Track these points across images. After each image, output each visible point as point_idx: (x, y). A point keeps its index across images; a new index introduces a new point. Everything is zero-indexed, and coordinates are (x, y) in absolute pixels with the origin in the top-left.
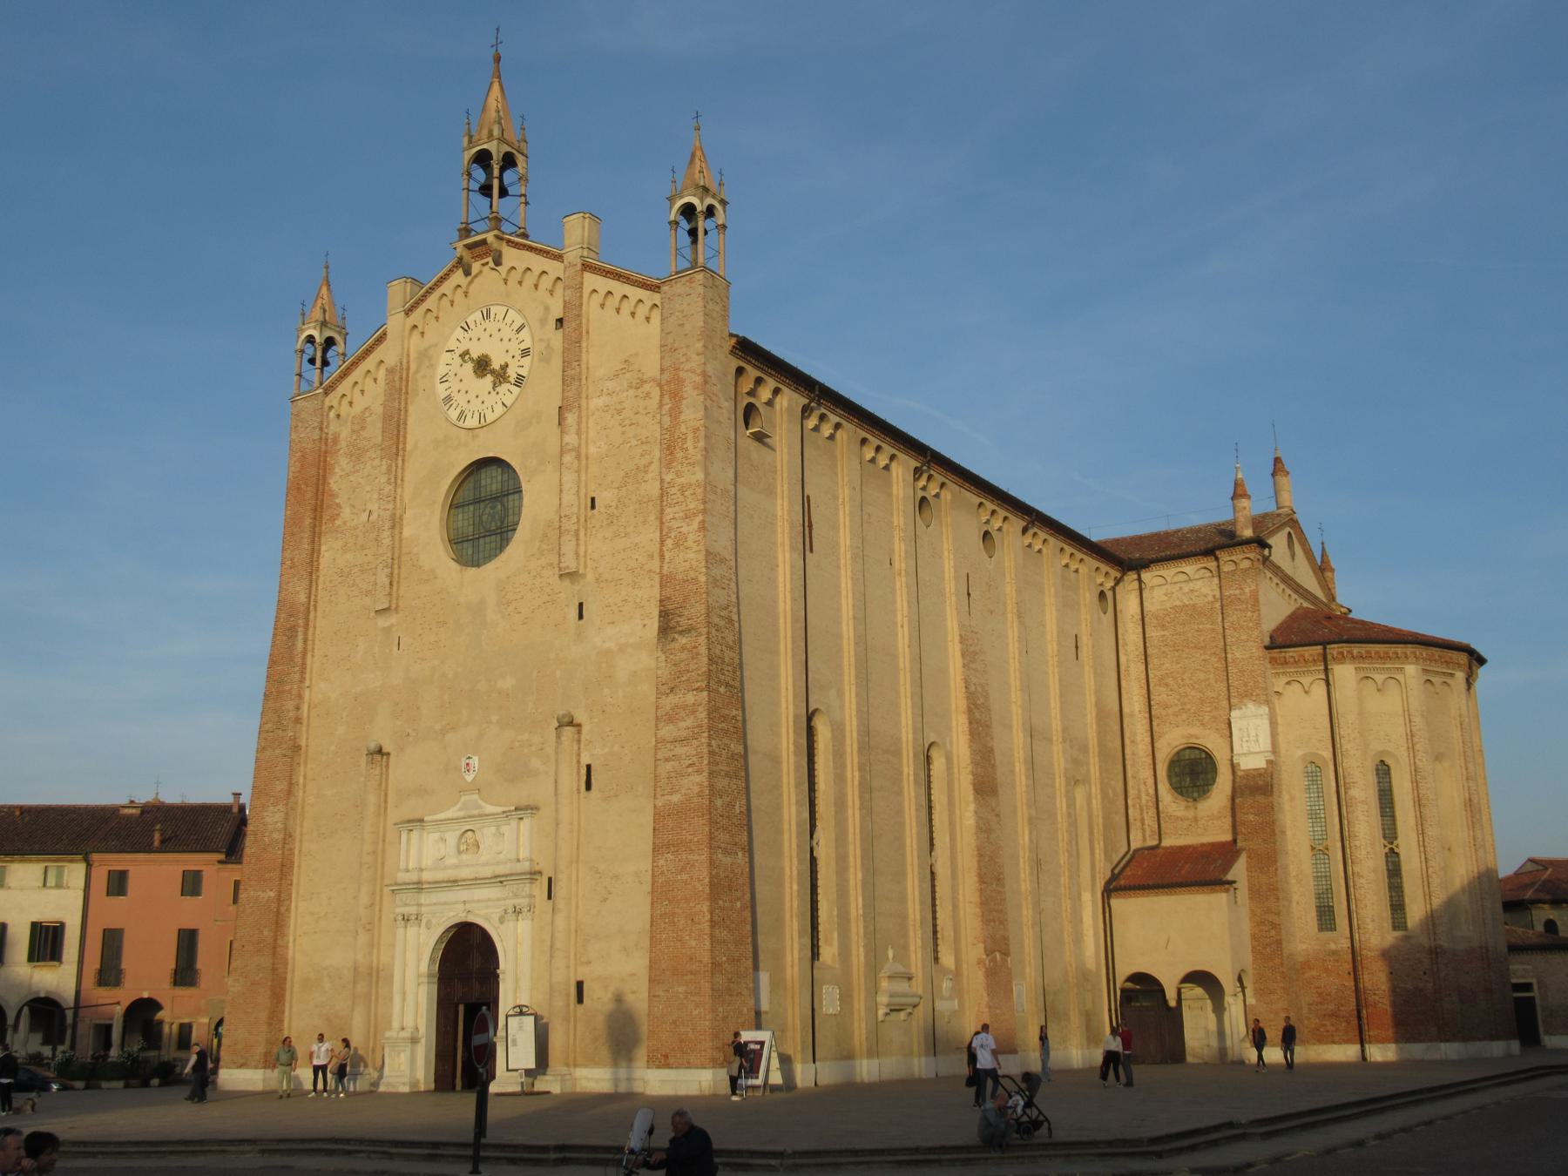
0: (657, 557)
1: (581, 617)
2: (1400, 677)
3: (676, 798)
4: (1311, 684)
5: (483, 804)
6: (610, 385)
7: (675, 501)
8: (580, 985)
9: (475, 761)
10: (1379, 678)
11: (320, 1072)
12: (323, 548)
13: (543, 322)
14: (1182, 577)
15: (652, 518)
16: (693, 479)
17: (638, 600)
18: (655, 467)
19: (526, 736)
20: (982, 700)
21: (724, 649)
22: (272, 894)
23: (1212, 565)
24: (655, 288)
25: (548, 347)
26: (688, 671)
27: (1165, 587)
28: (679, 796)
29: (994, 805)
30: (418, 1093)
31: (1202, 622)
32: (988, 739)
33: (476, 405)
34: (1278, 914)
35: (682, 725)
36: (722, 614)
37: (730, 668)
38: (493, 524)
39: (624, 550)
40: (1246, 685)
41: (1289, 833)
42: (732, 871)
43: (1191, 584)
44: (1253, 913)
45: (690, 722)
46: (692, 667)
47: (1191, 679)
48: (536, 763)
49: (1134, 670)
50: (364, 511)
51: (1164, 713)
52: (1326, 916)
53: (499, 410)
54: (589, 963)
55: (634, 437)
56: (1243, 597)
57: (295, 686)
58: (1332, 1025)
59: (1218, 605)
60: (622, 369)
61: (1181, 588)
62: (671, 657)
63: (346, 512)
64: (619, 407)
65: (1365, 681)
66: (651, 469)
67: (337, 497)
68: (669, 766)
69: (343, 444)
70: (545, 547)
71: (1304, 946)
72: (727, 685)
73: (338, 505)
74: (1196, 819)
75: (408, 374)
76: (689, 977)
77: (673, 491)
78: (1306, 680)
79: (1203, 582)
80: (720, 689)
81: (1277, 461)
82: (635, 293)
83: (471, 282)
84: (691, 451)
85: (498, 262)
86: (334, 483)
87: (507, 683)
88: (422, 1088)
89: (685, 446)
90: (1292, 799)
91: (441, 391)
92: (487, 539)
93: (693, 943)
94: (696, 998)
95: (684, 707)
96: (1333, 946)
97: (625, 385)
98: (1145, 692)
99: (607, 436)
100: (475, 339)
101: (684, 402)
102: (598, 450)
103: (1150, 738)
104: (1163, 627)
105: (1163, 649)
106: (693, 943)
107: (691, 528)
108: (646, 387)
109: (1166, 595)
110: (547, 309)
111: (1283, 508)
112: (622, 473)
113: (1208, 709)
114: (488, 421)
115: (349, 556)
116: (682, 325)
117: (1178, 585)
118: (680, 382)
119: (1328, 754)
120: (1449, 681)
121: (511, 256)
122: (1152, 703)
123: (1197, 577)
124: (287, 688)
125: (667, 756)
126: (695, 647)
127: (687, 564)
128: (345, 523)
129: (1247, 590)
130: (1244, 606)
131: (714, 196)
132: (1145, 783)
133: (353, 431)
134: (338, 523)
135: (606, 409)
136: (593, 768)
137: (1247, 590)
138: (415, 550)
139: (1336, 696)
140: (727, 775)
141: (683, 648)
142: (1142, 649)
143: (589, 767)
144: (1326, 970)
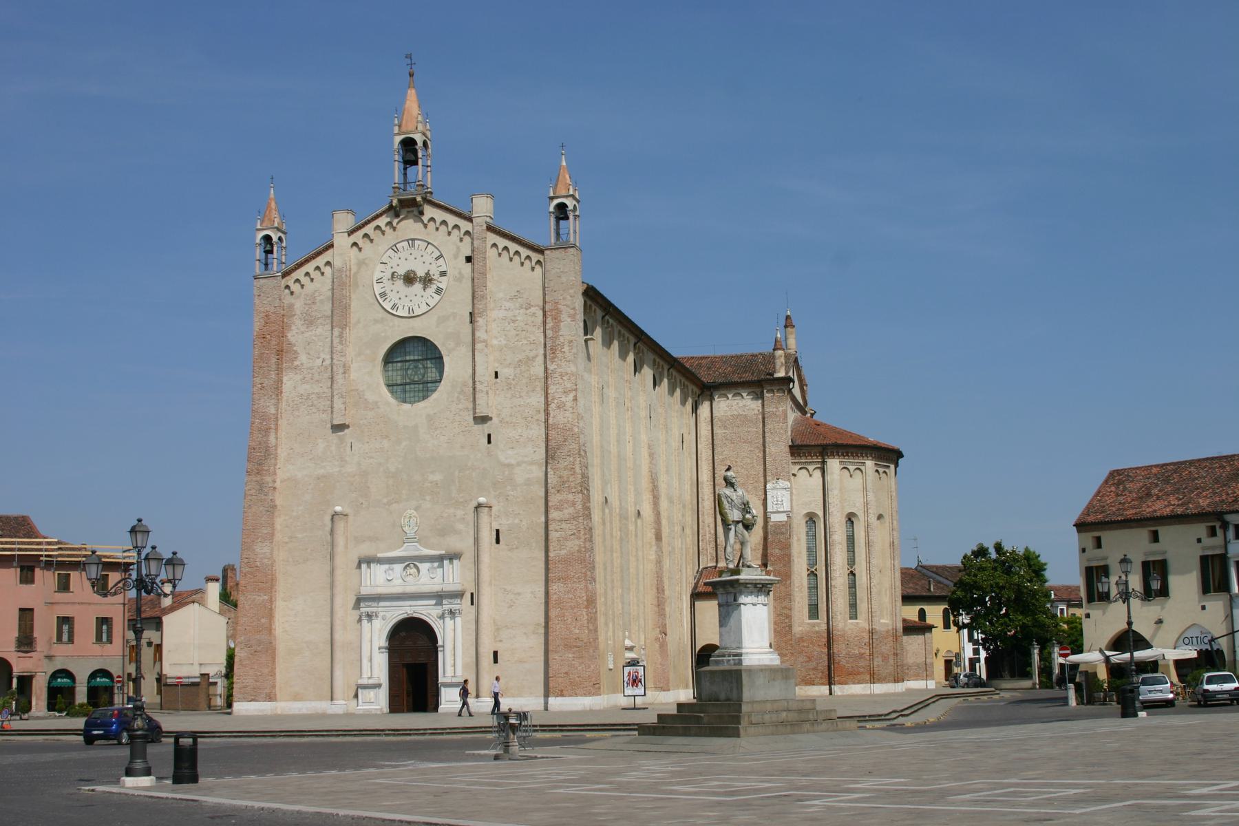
0: (543, 414)
1: (489, 442)
2: (863, 468)
3: (563, 552)
4: (814, 470)
5: (421, 548)
6: (508, 304)
8: (495, 654)
10: (852, 468)
11: (14, 711)
12: (285, 379)
13: (456, 257)
15: (538, 389)
16: (569, 370)
18: (540, 359)
19: (452, 510)
22: (266, 597)
24: (541, 251)
25: (460, 273)
28: (565, 551)
30: (383, 714)
33: (406, 302)
34: (790, 609)
35: (566, 511)
38: (416, 377)
39: (519, 406)
41: (796, 560)
45: (571, 510)
46: (571, 479)
48: (460, 526)
49: (705, 453)
50: (318, 358)
52: (814, 612)
53: (424, 308)
54: (501, 641)
55: (525, 338)
56: (777, 413)
57: (272, 468)
58: (814, 674)
59: (760, 417)
60: (515, 296)
61: (738, 404)
62: (557, 472)
63: (303, 358)
64: (513, 318)
65: (844, 470)
66: (537, 359)
67: (295, 346)
68: (558, 535)
69: (298, 312)
70: (461, 397)
71: (801, 628)
73: (296, 352)
75: (350, 273)
76: (576, 649)
77: (556, 375)
78: (811, 468)
81: (788, 317)
82: (525, 252)
84: (567, 354)
85: (422, 213)
86: (291, 336)
87: (437, 477)
88: (385, 712)
89: (563, 350)
90: (799, 540)
91: (378, 289)
92: (412, 386)
93: (577, 631)
94: (580, 661)
95: (567, 502)
96: (817, 628)
97: (518, 305)
98: (711, 468)
99: (505, 335)
100: (403, 259)
101: (562, 324)
102: (500, 343)
103: (713, 498)
104: (725, 428)
105: (724, 442)
106: (577, 631)
108: (533, 310)
110: (458, 248)
111: (790, 349)
112: (517, 359)
114: (416, 314)
115: (307, 386)
118: (559, 311)
119: (821, 514)
120: (887, 470)
121: (429, 212)
124: (266, 468)
125: (557, 528)
128: (302, 364)
129: (781, 409)
132: (709, 526)
133: (305, 304)
134: (296, 363)
135: (504, 319)
136: (500, 531)
137: (781, 409)
138: (361, 389)
139: (829, 478)
142: (711, 441)
143: (498, 531)
144: (812, 643)
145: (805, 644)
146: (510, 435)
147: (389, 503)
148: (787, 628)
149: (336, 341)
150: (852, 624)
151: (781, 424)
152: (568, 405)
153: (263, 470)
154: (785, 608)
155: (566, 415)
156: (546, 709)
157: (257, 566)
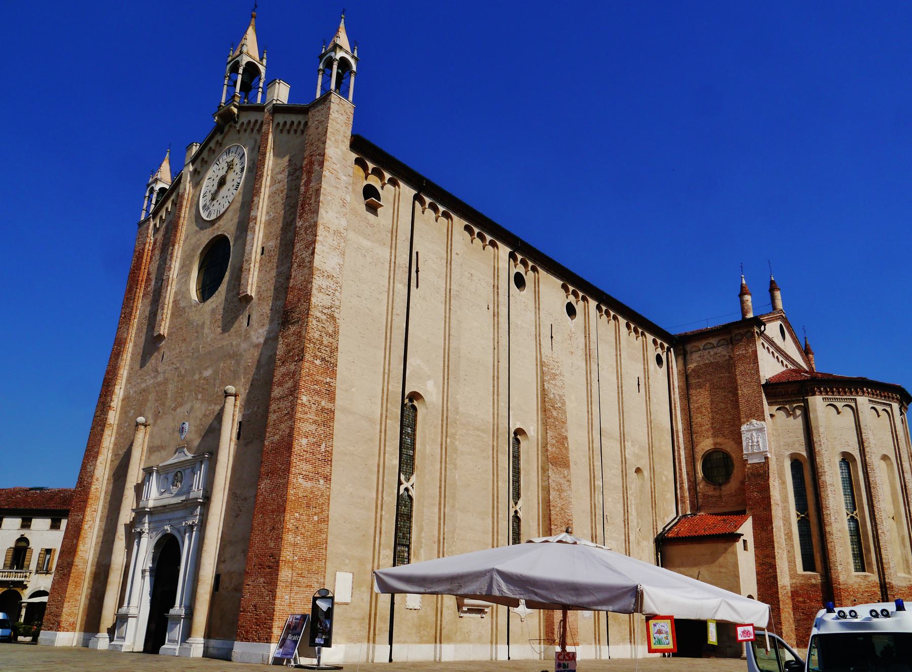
3: (277, 437)
7: (301, 238)
9: (187, 426)
14: (709, 346)
17: (278, 308)
20: (559, 405)
21: (323, 334)
23: (728, 337)
26: (294, 349)
27: (699, 352)
29: (566, 472)
31: (722, 373)
32: (563, 430)
35: (287, 386)
36: (324, 311)
37: (327, 349)
40: (750, 410)
42: (312, 492)
43: (715, 350)
44: (756, 556)
47: (716, 408)
51: (699, 430)
61: (709, 353)
62: (286, 340)
72: (323, 359)
74: (720, 497)
79: (723, 348)
80: (315, 361)
81: (772, 282)
83: (224, 138)
87: (208, 373)
93: (272, 545)
96: (813, 581)
104: (699, 377)
107: (307, 254)
109: (700, 357)
113: (727, 426)
116: (317, 128)
117: (708, 351)
122: (692, 423)
123: (719, 345)
126: (300, 332)
127: (303, 278)
129: (750, 350)
130: (748, 360)
131: (347, 52)
137: (750, 350)
140: (315, 422)
141: (293, 334)
144: (809, 598)
145: (801, 599)
146: (264, 311)
147: (175, 409)
148: (772, 580)
149: (169, 257)
150: (858, 576)
151: (752, 365)
152: (307, 259)
153: (108, 391)
154: (767, 556)
155: (304, 272)
156: (509, 658)
157: (84, 486)
